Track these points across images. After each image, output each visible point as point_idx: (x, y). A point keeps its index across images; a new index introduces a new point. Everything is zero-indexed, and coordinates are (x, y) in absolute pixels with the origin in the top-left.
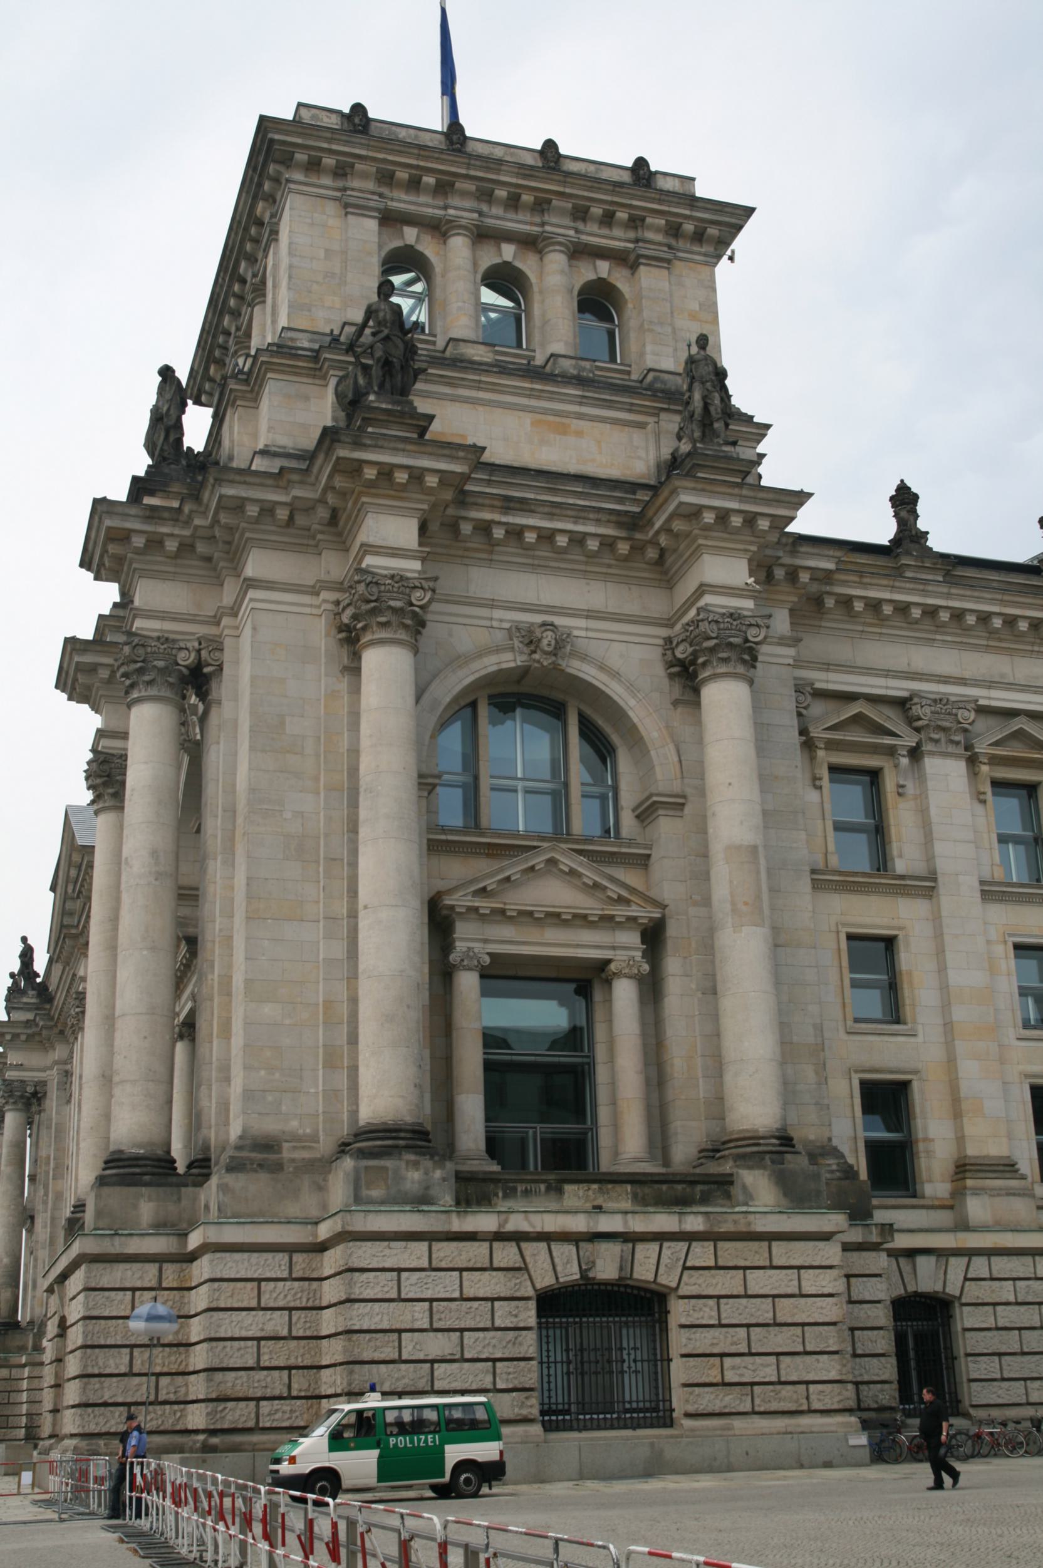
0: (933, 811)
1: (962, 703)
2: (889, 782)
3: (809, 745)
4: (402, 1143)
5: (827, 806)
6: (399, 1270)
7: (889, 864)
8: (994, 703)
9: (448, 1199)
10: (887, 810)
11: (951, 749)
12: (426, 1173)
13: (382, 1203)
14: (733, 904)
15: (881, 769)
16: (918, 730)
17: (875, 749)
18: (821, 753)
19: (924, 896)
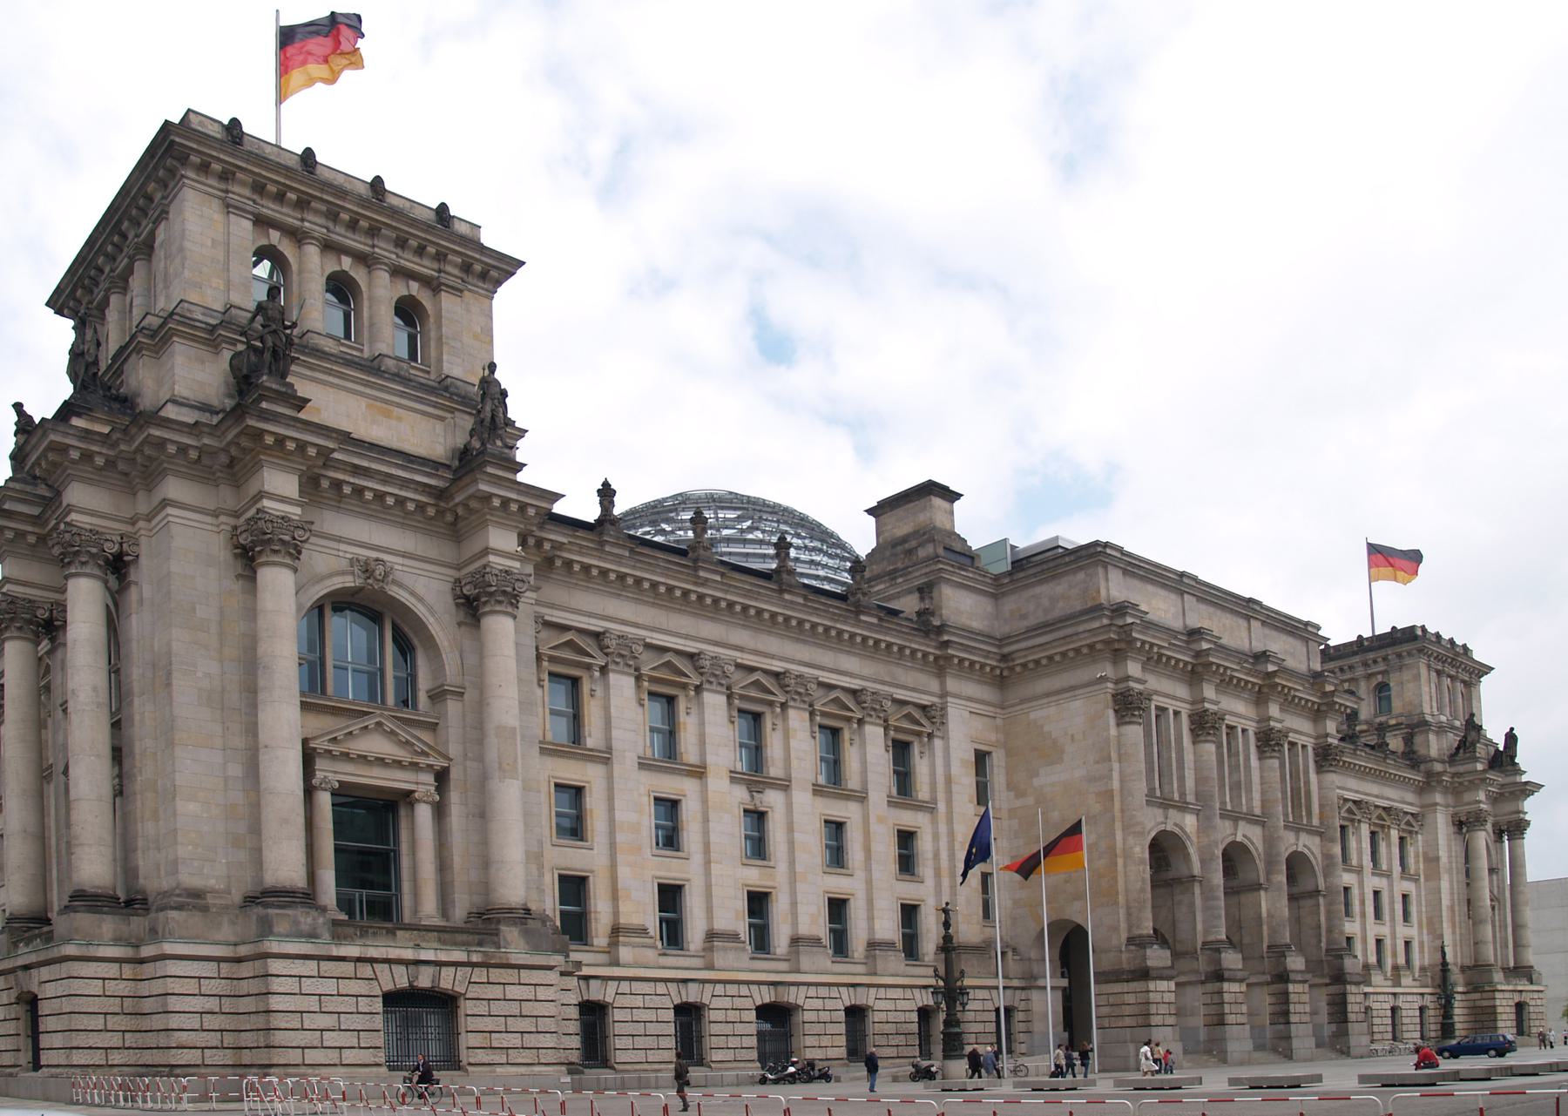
0: (613, 710)
1: (636, 640)
2: (586, 687)
3: (539, 657)
4: (297, 900)
5: (546, 699)
6: (300, 977)
7: (582, 740)
8: (654, 642)
9: (327, 936)
10: (583, 705)
11: (626, 669)
12: (314, 919)
13: (287, 936)
14: (500, 764)
15: (581, 678)
16: (607, 654)
17: (578, 665)
18: (545, 664)
19: (602, 763)
